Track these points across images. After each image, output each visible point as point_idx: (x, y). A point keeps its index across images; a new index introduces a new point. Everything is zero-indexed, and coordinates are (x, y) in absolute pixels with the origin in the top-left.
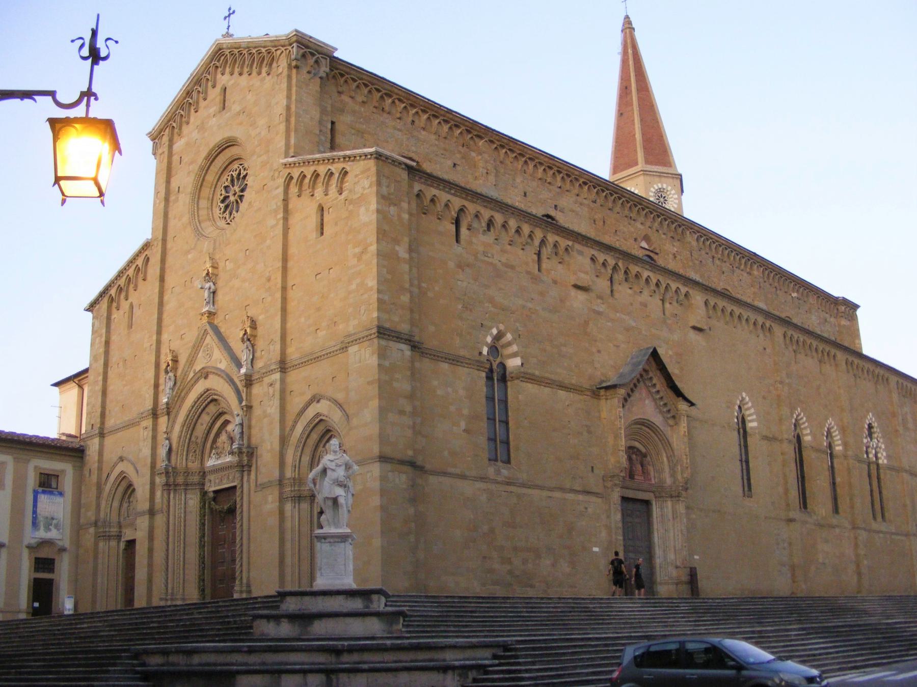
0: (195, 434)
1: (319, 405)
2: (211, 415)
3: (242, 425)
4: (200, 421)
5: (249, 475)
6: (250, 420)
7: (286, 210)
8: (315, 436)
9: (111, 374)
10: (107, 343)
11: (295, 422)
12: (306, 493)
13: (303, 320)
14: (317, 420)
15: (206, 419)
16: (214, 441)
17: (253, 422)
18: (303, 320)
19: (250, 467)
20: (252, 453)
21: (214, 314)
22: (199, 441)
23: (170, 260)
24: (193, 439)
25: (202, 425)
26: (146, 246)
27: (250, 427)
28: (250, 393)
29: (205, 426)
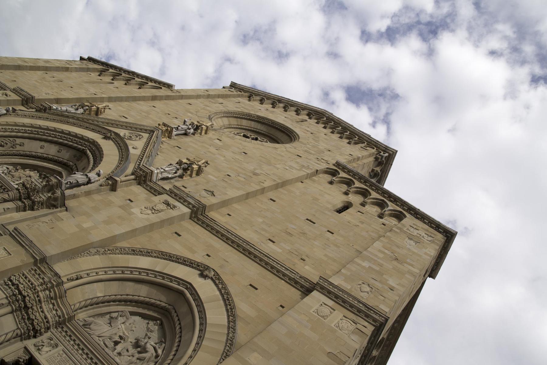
0: (26, 141)
1: (201, 280)
2: (59, 155)
3: (89, 182)
4: (46, 144)
5: (18, 210)
6: (98, 191)
7: (309, 176)
8: (142, 292)
9: (40, 73)
10: (67, 69)
11: (148, 253)
12: (37, 316)
13: (260, 220)
14: (174, 285)
15: (52, 150)
16: (24, 167)
17: (96, 197)
18: (260, 220)
19: (32, 209)
20: (55, 207)
21: (170, 137)
22: (18, 148)
23: (172, 102)
24: (18, 141)
25: (41, 148)
26: (169, 86)
27: (88, 194)
28: (131, 185)
29: (41, 151)
